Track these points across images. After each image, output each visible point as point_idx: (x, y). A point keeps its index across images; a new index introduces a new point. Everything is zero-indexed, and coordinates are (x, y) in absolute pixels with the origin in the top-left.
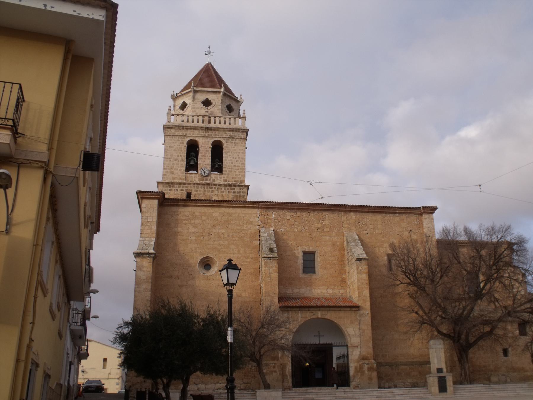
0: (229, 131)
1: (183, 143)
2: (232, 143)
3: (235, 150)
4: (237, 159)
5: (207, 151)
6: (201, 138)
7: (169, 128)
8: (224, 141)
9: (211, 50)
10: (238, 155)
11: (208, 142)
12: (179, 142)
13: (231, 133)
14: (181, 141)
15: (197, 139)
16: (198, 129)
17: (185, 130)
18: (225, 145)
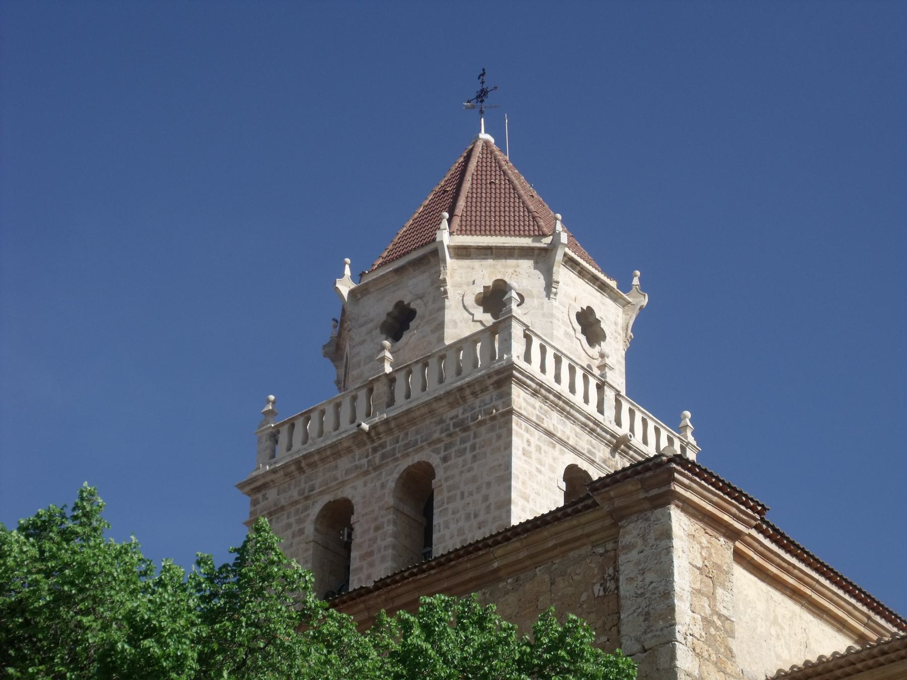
0: (452, 406)
1: (301, 532)
2: (462, 452)
3: (474, 479)
4: (481, 518)
5: (377, 529)
6: (359, 483)
7: (258, 490)
8: (435, 460)
9: (488, 85)
10: (486, 498)
11: (383, 486)
12: (289, 533)
13: (458, 411)
14: (295, 528)
15: (347, 492)
16: (349, 450)
17: (309, 471)
18: (440, 474)
